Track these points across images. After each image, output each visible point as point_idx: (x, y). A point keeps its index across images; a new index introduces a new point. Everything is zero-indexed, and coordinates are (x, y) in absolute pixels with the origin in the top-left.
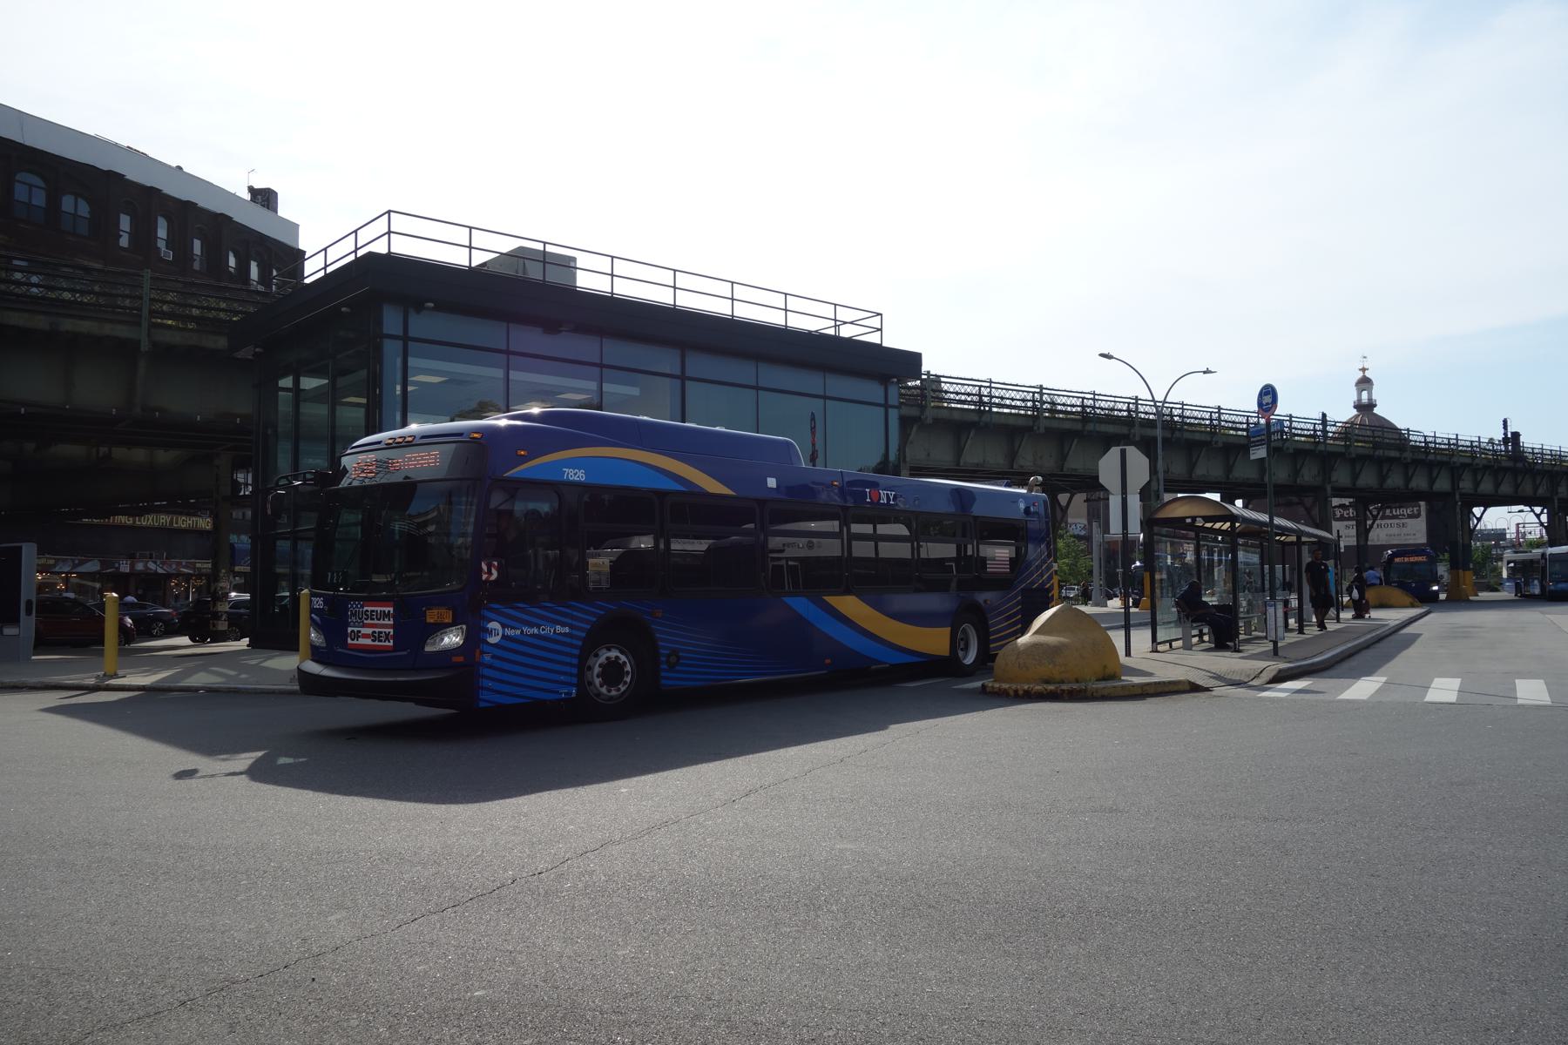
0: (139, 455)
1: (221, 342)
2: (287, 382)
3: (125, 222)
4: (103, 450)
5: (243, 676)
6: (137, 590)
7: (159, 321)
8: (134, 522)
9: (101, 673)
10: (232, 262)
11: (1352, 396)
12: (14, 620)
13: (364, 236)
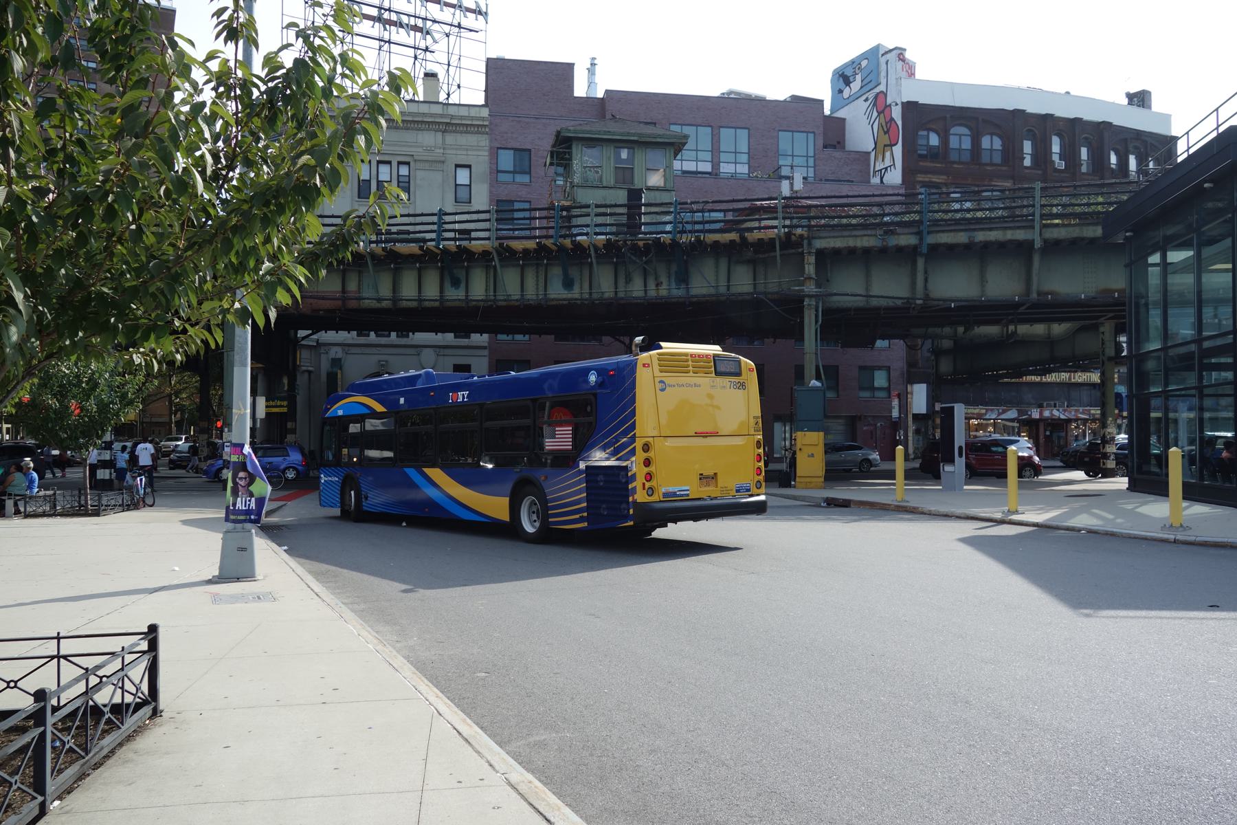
0: (1039, 329)
1: (1098, 231)
2: (1155, 258)
3: (1027, 147)
4: (1011, 328)
5: (1119, 521)
6: (1045, 432)
7: (1049, 222)
8: (1041, 379)
9: (1006, 509)
10: (1113, 159)
12: (951, 461)
13: (1224, 113)
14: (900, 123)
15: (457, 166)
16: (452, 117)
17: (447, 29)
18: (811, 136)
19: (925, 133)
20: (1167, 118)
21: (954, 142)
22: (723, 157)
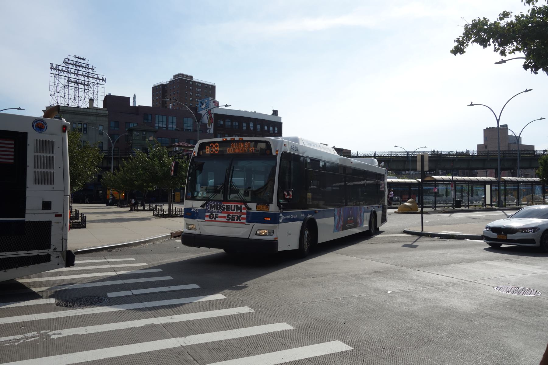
3: (244, 125)
10: (266, 128)
14: (213, 118)
15: (99, 125)
16: (99, 113)
17: (94, 83)
18: (192, 119)
19: (219, 121)
20: (280, 118)
21: (226, 123)
22: (169, 123)
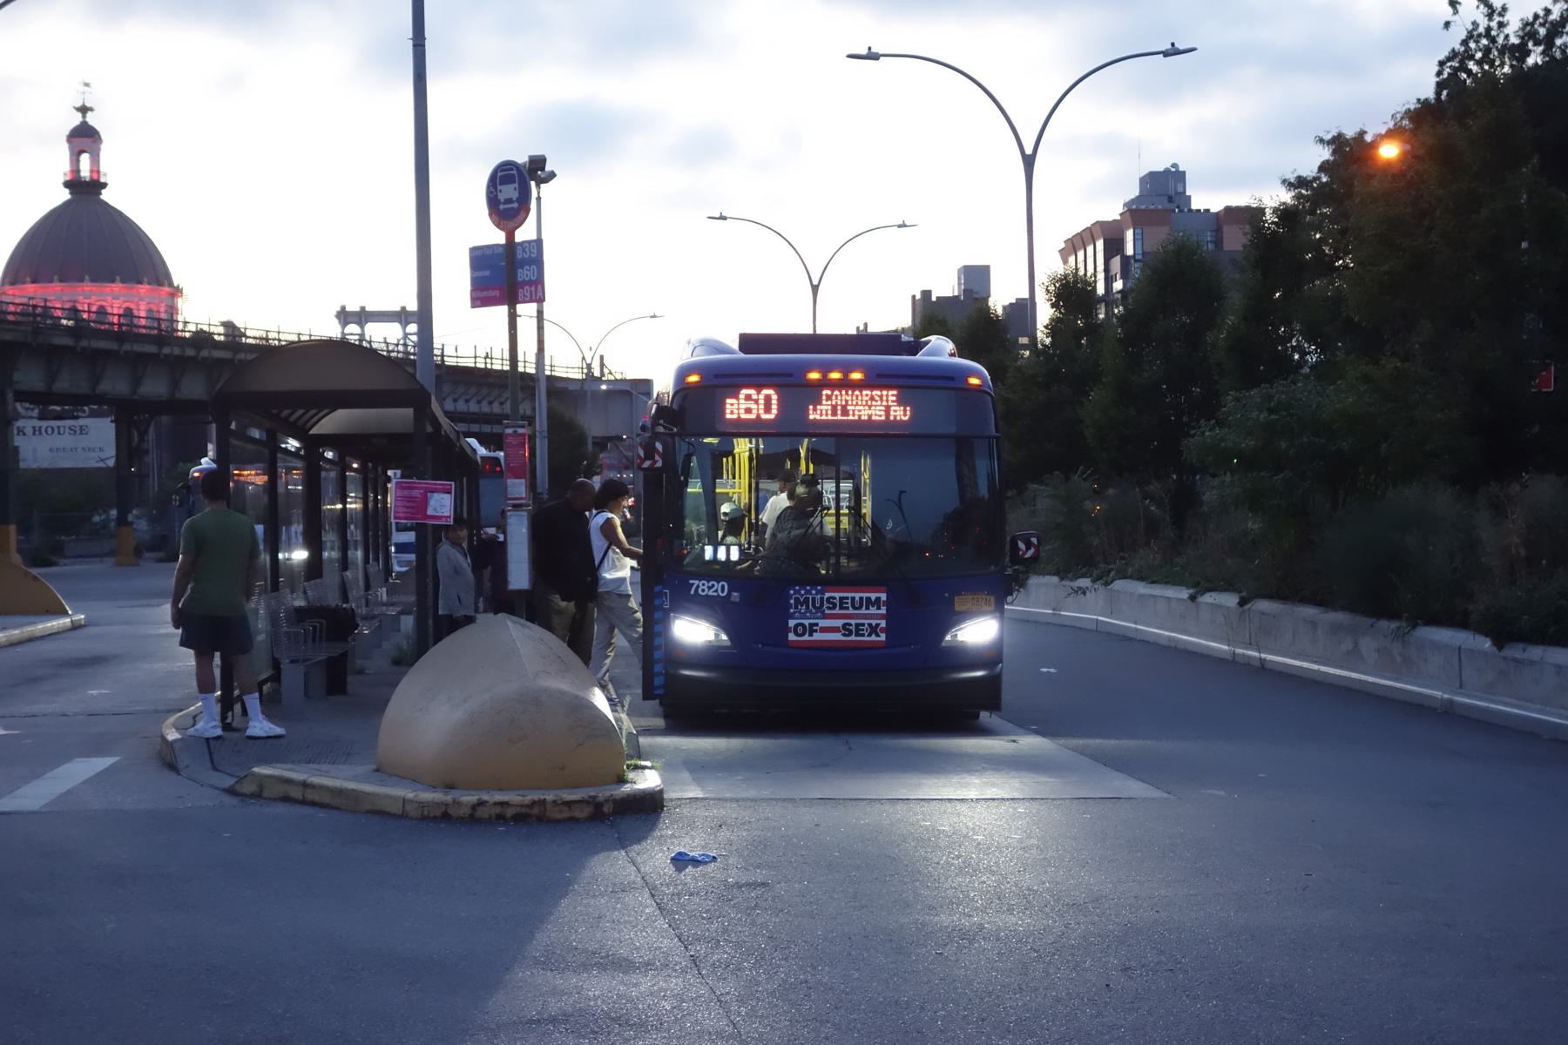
11: (58, 163)
